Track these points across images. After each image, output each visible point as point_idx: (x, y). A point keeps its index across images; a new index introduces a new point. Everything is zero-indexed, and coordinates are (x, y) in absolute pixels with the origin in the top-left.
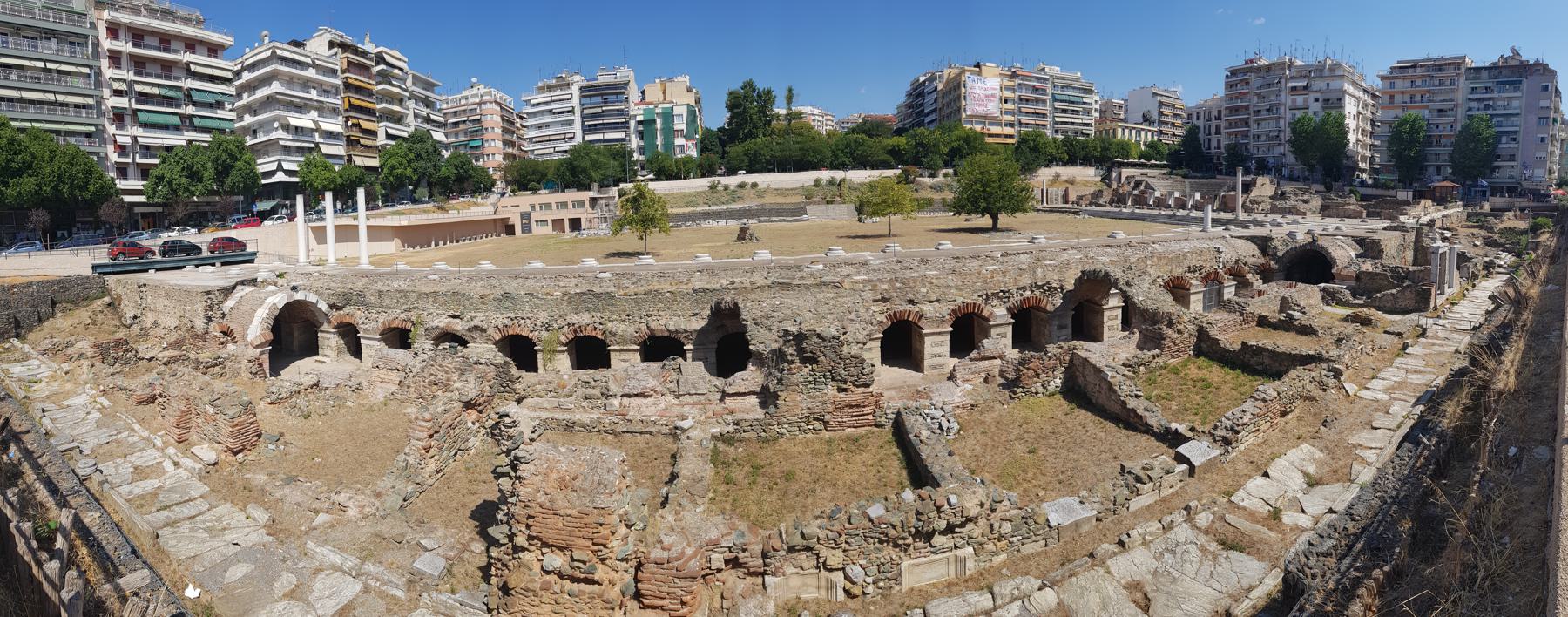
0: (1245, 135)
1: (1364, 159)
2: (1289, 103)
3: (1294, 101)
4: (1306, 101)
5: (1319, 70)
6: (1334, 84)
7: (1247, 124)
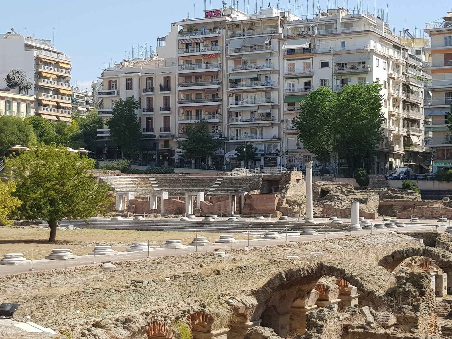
0: (215, 112)
1: (397, 137)
2: (285, 71)
3: (291, 67)
4: (307, 66)
5: (327, 25)
6: (353, 43)
7: (215, 95)
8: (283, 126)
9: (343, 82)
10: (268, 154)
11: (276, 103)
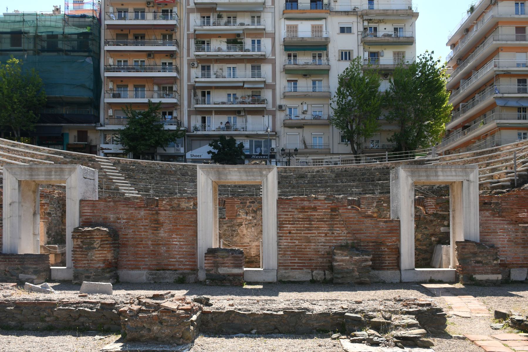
2: (282, 33)
3: (292, 29)
4: (316, 30)
8: (280, 116)
9: (374, 56)
10: (257, 155)
11: (269, 81)
